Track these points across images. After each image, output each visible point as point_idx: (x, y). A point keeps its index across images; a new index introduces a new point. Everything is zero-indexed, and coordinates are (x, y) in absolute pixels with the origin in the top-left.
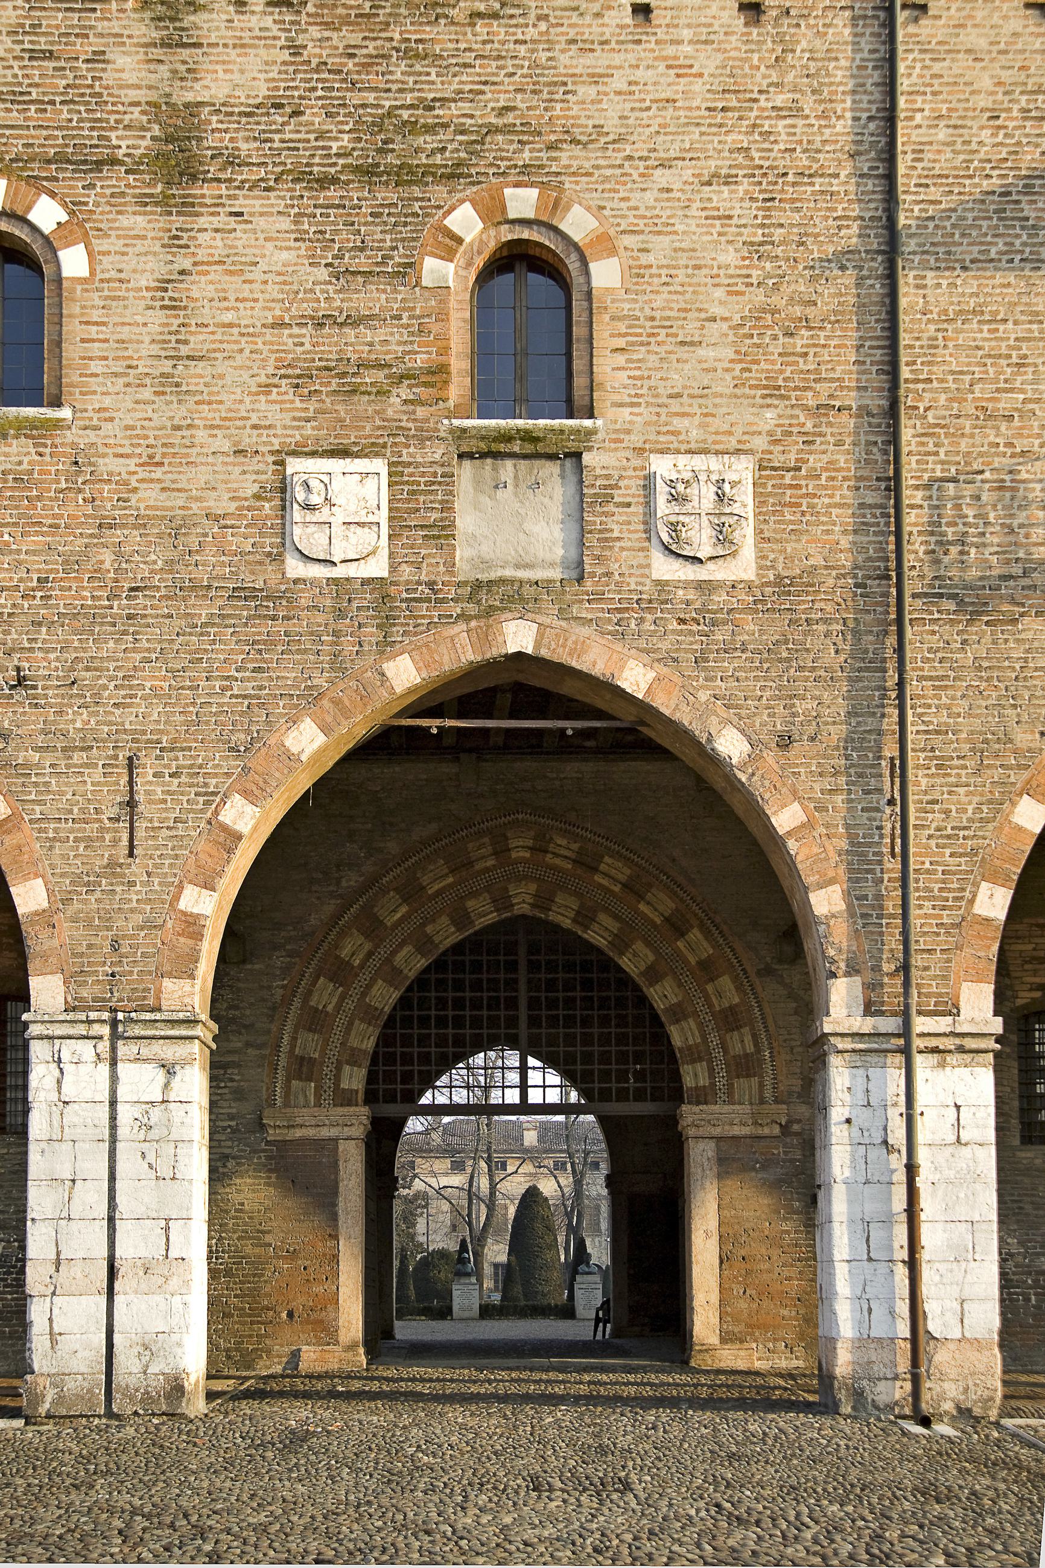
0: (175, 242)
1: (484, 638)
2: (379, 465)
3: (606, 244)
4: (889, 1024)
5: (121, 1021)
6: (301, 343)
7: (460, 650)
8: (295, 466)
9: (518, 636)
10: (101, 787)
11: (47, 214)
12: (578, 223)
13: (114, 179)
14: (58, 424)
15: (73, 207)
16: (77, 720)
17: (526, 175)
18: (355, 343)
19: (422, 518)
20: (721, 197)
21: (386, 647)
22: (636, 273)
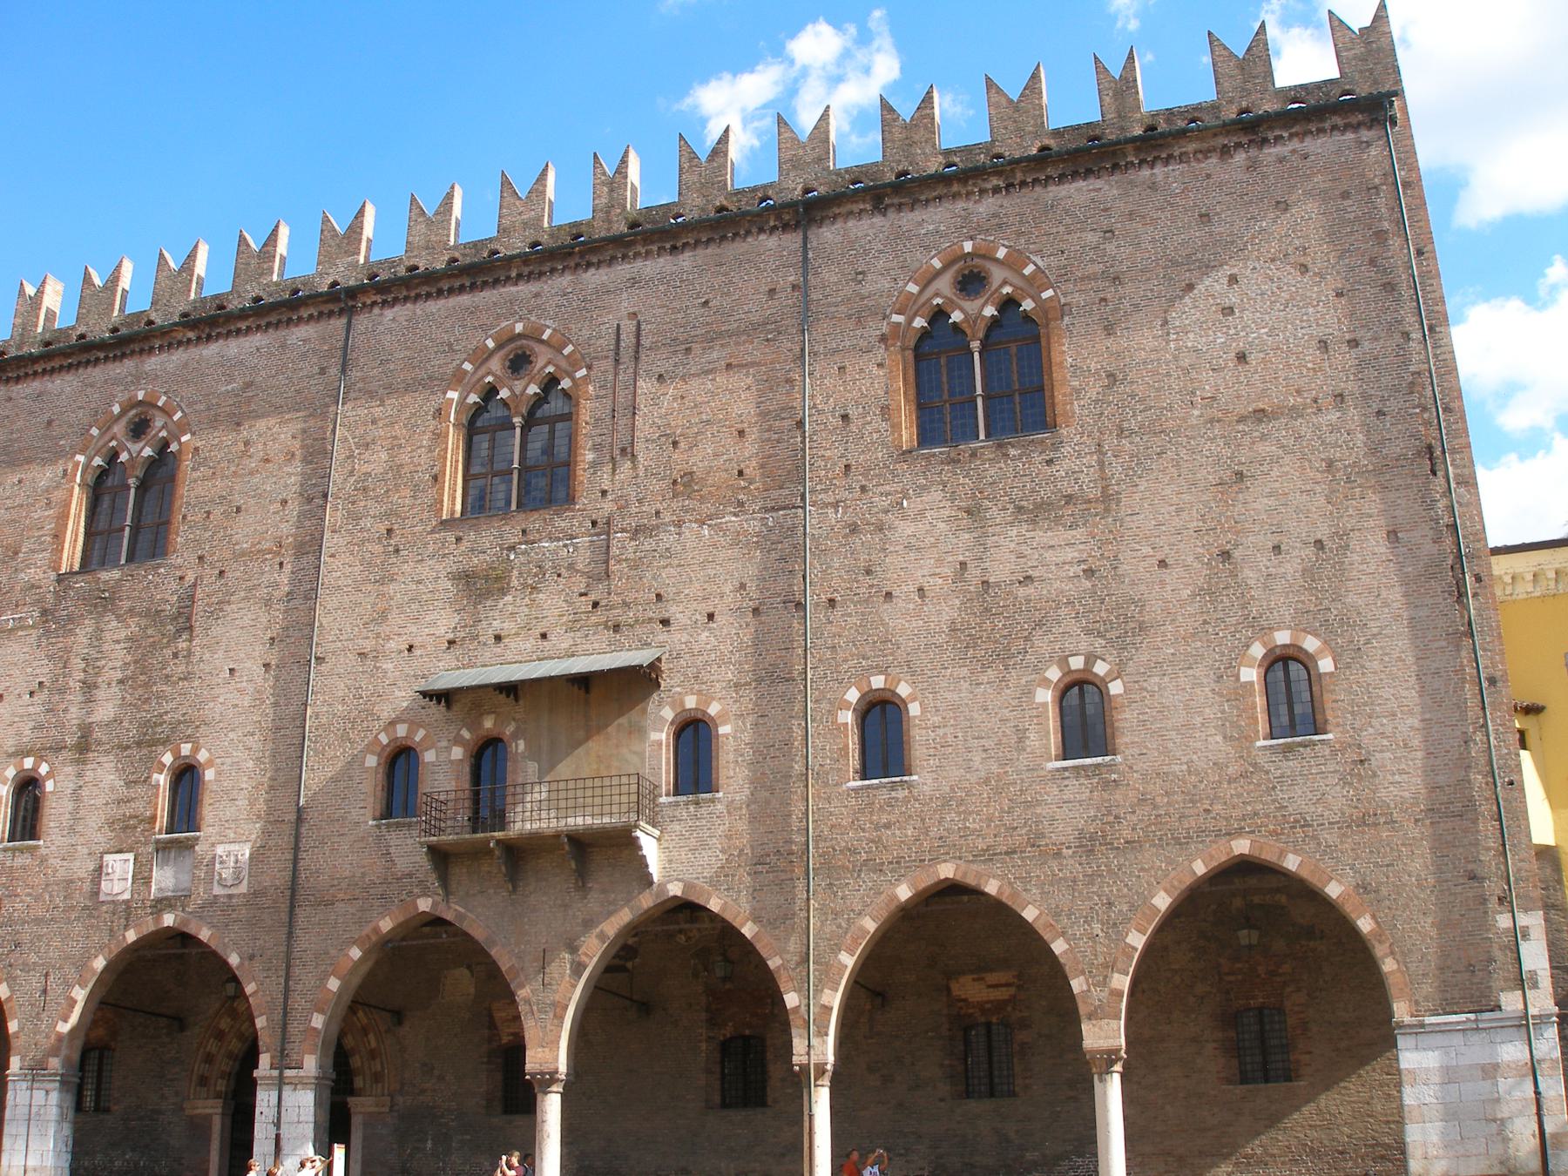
0: (79, 775)
1: (158, 919)
2: (131, 856)
3: (210, 763)
4: (275, 1073)
5: (36, 1071)
6: (117, 812)
7: (149, 926)
8: (107, 858)
9: (169, 920)
10: (36, 982)
11: (44, 769)
12: (203, 756)
13: (65, 754)
14: (38, 847)
15: (51, 766)
16: (33, 958)
17: (188, 739)
18: (127, 810)
19: (142, 877)
20: (250, 741)
21: (126, 928)
22: (219, 773)
